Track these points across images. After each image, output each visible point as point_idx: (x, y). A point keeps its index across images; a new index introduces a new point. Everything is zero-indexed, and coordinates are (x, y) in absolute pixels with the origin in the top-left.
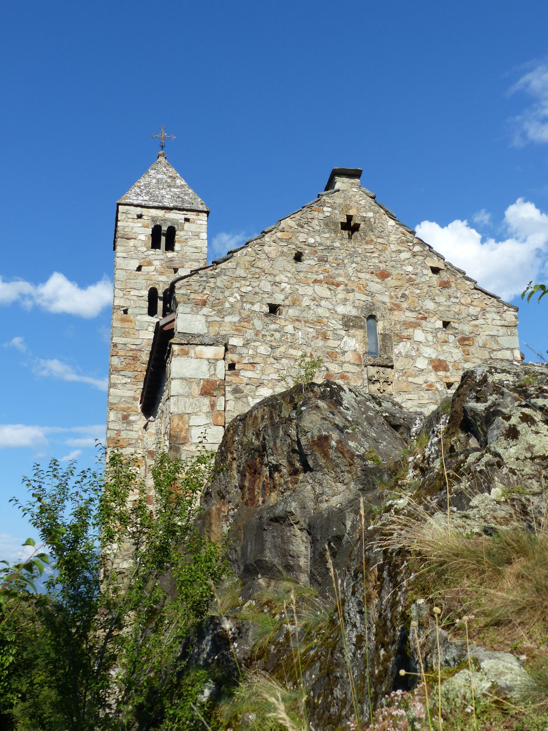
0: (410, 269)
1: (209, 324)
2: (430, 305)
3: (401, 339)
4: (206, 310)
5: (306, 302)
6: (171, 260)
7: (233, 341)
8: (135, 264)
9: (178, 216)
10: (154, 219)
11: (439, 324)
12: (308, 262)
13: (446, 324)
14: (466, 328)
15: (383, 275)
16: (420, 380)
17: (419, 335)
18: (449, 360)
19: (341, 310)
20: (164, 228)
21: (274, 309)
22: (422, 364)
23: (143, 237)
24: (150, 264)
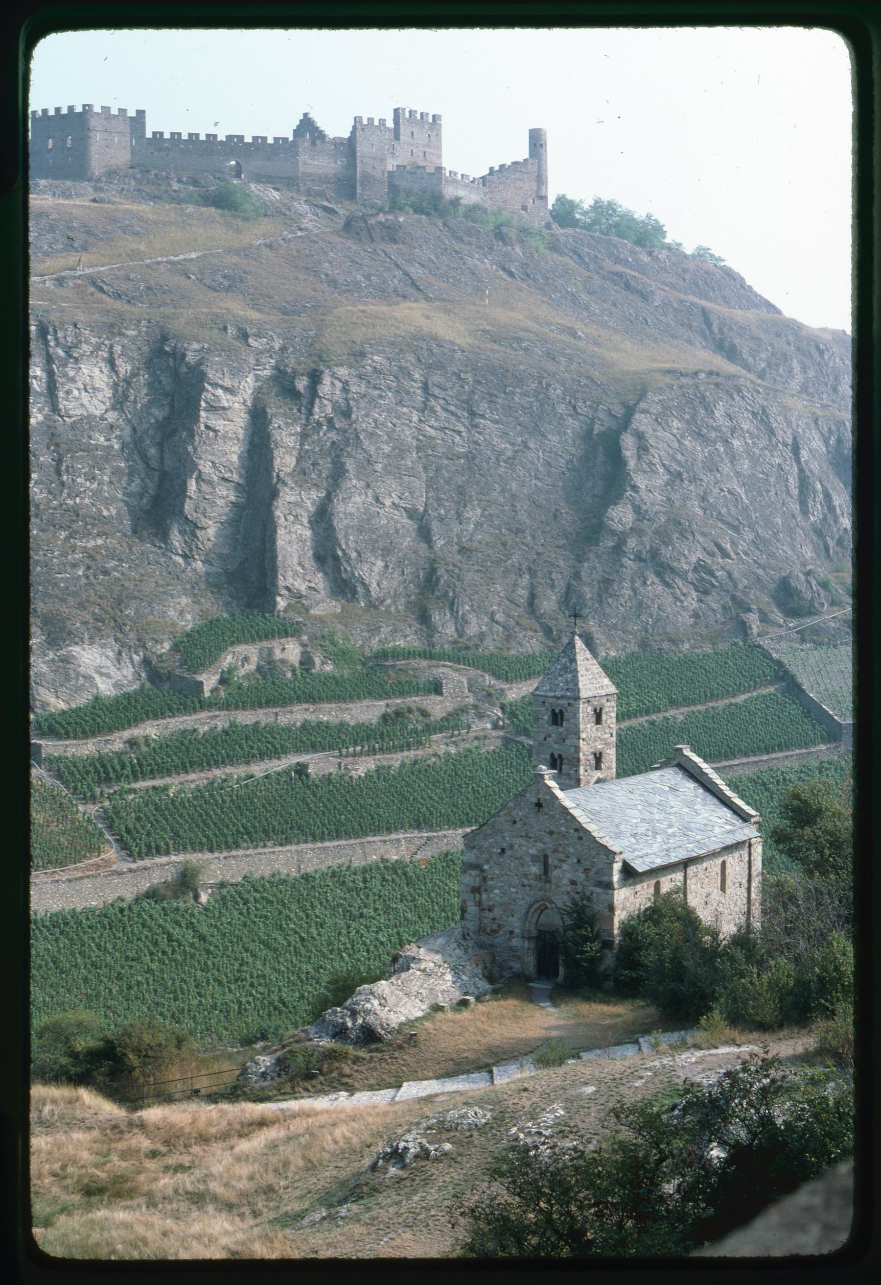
0: (564, 829)
1: (477, 858)
2: (572, 850)
3: (556, 867)
4: (475, 851)
5: (516, 847)
6: (561, 734)
7: (486, 867)
8: (542, 736)
9: (564, 702)
10: (551, 704)
11: (575, 860)
12: (518, 825)
13: (579, 861)
14: (587, 864)
15: (551, 833)
16: (563, 889)
17: (565, 866)
18: (579, 880)
19: (531, 851)
20: (557, 711)
21: (503, 850)
22: (565, 881)
23: (546, 718)
24: (550, 736)
